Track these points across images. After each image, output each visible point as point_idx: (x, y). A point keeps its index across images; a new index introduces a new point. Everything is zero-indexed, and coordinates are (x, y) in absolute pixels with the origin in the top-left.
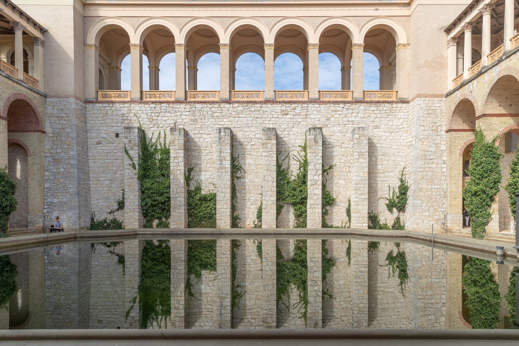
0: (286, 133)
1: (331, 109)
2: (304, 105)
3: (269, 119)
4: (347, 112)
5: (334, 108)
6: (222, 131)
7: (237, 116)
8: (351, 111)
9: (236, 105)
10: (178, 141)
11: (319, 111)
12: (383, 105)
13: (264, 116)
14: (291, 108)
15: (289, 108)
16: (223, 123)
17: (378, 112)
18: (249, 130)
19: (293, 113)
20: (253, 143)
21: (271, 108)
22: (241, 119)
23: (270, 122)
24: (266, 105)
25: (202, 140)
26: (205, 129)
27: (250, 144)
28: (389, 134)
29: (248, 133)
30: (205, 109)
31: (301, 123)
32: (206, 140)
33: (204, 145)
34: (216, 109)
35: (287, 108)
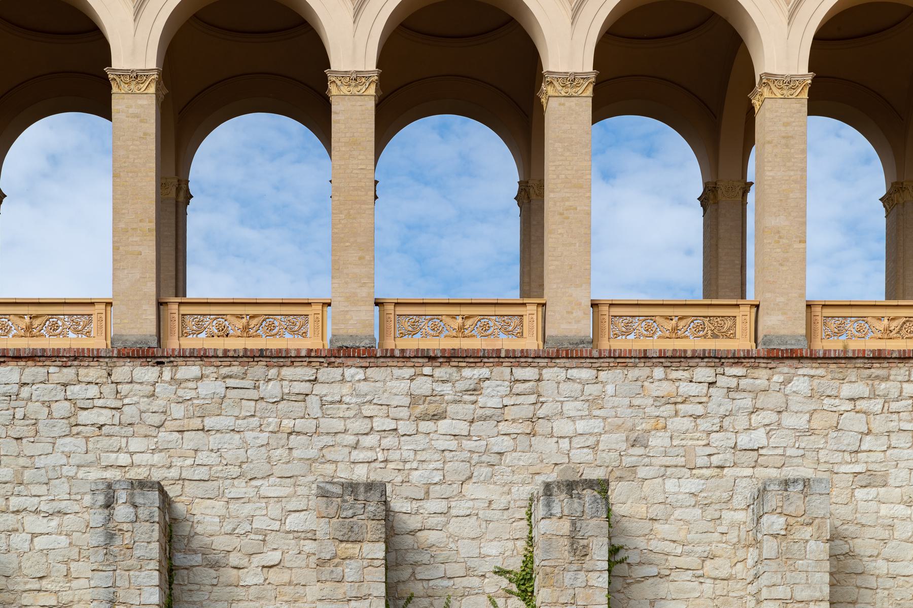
0: (433, 505)
1: (655, 389)
2: (520, 373)
3: (350, 439)
4: (728, 405)
5: (666, 388)
6: (122, 496)
7: (196, 423)
8: (747, 402)
9: (191, 370)
11: (595, 402)
13: (327, 424)
14: (461, 386)
15: (447, 388)
16: (123, 459)
17: (876, 405)
18: (251, 492)
19: (466, 410)
20: (274, 557)
21: (364, 387)
22: (214, 440)
23: (358, 455)
24: (335, 373)
25: (19, 541)
26: (35, 490)
27: (257, 560)
29: (247, 509)
30: (39, 391)
31: (508, 459)
32: (39, 543)
33: (31, 566)
34: (93, 391)
35: (439, 388)
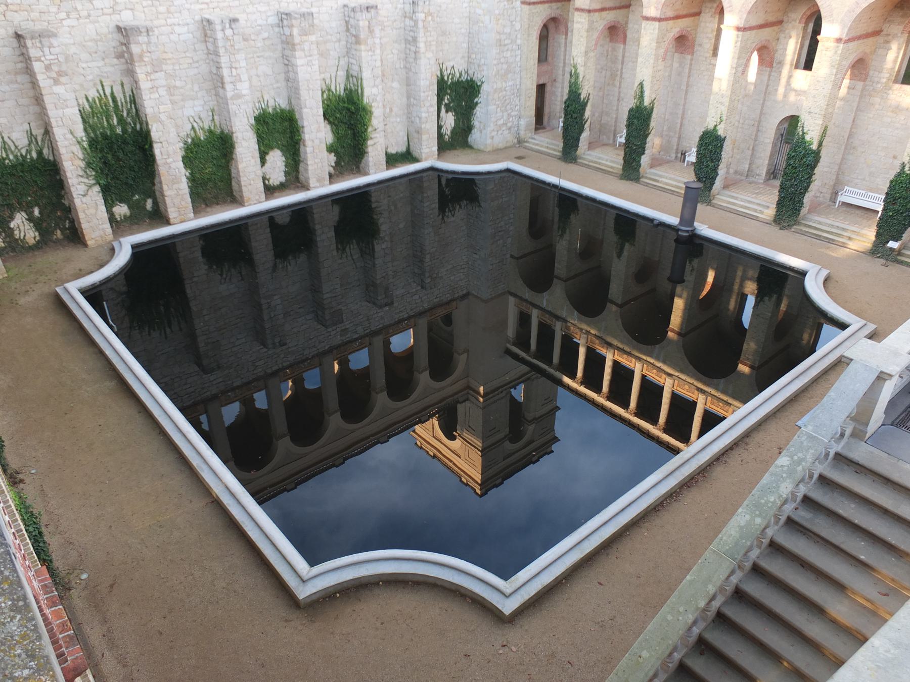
10: (149, 54)
20: (266, 35)
26: (176, 15)
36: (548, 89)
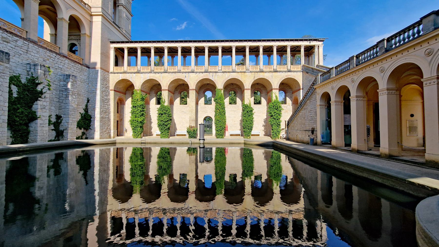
4: (57, 61)
5: (49, 54)
12: (78, 64)
15: (10, 38)
17: (75, 68)
28: (80, 83)
31: (22, 55)
35: (8, 37)
36: (119, 123)
